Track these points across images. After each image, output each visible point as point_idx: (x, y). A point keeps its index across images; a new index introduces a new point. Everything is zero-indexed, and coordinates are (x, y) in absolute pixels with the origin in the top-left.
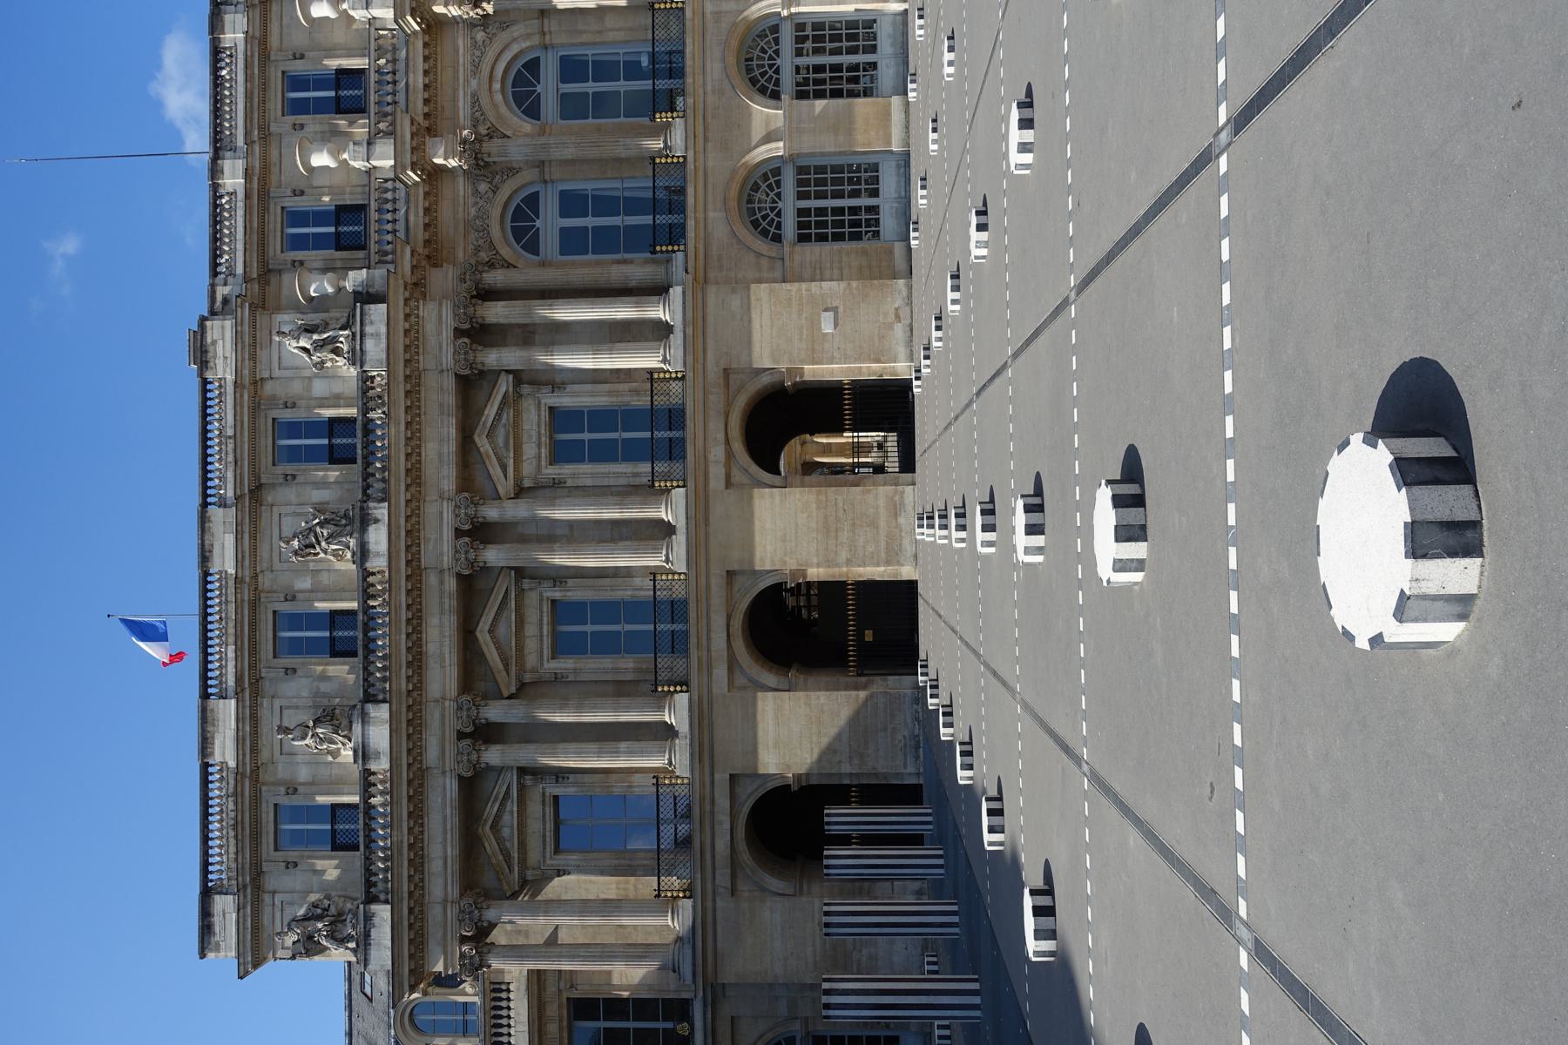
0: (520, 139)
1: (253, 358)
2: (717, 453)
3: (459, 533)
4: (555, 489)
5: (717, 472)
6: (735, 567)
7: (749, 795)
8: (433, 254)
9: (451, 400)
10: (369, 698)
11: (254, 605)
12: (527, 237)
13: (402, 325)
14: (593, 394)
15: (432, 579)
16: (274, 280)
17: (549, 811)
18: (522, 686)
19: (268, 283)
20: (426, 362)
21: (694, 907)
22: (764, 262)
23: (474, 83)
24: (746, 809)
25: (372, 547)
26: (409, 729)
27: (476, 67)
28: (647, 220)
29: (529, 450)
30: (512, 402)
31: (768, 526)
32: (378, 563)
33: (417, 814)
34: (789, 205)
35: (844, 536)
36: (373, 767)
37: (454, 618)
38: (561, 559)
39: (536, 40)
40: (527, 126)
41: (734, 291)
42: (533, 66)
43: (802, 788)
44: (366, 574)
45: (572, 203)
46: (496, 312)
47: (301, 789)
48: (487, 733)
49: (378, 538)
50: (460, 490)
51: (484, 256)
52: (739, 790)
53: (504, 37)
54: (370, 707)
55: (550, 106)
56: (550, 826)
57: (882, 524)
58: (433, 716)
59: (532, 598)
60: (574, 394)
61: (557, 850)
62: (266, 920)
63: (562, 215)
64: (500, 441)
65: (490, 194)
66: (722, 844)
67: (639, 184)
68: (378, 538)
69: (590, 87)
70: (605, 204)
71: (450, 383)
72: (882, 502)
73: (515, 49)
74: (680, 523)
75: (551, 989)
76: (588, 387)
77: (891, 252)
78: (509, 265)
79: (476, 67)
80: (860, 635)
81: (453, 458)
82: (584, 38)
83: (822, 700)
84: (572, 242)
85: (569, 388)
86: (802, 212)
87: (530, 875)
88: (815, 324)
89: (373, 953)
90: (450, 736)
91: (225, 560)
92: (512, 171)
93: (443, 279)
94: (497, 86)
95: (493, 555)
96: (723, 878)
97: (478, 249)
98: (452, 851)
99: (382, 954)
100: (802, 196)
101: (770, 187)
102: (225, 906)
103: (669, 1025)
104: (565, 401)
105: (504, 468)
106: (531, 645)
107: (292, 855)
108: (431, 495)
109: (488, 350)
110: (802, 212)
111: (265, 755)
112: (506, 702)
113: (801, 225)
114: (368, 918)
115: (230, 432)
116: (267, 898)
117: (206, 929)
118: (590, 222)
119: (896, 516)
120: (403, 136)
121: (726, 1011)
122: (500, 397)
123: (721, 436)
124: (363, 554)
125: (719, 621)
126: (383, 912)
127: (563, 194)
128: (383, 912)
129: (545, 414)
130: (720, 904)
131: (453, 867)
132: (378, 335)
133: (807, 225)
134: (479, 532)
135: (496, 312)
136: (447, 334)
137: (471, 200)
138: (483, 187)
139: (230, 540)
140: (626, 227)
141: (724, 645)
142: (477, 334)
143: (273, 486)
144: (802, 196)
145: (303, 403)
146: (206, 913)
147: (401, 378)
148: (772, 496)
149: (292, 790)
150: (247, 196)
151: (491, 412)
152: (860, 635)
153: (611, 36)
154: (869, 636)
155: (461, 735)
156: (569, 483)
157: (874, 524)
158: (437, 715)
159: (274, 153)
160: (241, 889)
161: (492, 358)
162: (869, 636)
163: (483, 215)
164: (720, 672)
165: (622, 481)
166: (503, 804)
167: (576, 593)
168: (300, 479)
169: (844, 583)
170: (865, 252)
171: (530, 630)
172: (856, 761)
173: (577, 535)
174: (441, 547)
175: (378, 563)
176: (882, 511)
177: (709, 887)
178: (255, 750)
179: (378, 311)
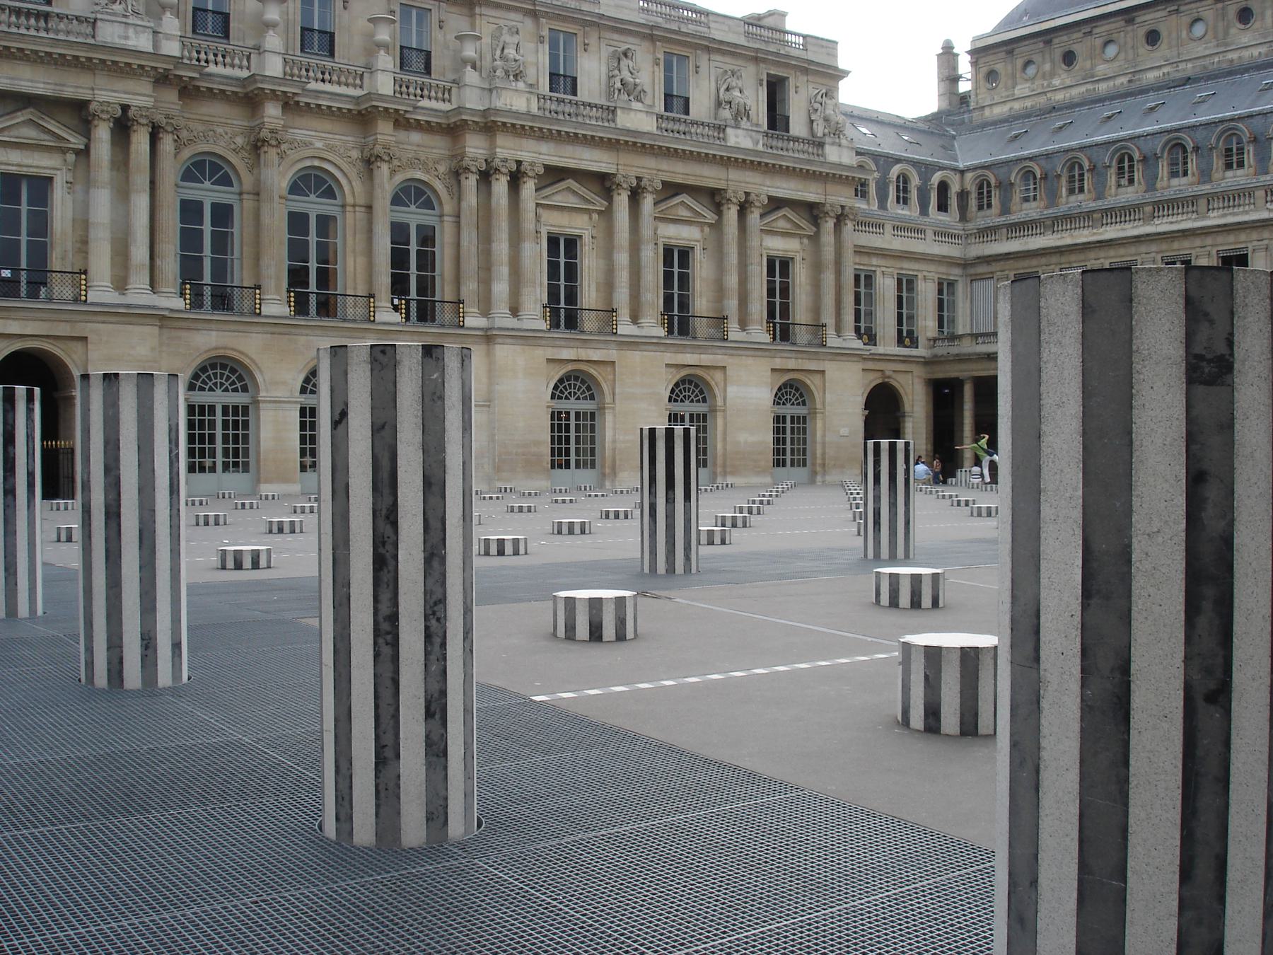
0: (278, 177)
8: (189, 91)
9: (68, 92)
13: (135, 62)
20: (101, 80)
23: (319, 144)
27: (330, 148)
28: (207, 279)
34: (219, 398)
39: (349, 200)
40: (285, 184)
41: (153, 349)
42: (330, 193)
45: (222, 214)
46: (140, 141)
51: (184, 134)
53: (353, 173)
63: (214, 205)
65: (233, 146)
67: (240, 275)
70: (222, 243)
71: (84, 95)
73: (343, 181)
78: (175, 156)
84: (190, 210)
86: (212, 409)
94: (316, 163)
100: (225, 409)
101: (233, 383)
109: (109, 132)
110: (212, 409)
113: (202, 407)
118: (207, 228)
120: (285, 85)
122: (65, 135)
129: (47, 173)
132: (127, 38)
133: (236, 413)
135: (140, 141)
138: (240, 141)
140: (201, 258)
147: (90, 55)
151: (52, 126)
161: (103, 133)
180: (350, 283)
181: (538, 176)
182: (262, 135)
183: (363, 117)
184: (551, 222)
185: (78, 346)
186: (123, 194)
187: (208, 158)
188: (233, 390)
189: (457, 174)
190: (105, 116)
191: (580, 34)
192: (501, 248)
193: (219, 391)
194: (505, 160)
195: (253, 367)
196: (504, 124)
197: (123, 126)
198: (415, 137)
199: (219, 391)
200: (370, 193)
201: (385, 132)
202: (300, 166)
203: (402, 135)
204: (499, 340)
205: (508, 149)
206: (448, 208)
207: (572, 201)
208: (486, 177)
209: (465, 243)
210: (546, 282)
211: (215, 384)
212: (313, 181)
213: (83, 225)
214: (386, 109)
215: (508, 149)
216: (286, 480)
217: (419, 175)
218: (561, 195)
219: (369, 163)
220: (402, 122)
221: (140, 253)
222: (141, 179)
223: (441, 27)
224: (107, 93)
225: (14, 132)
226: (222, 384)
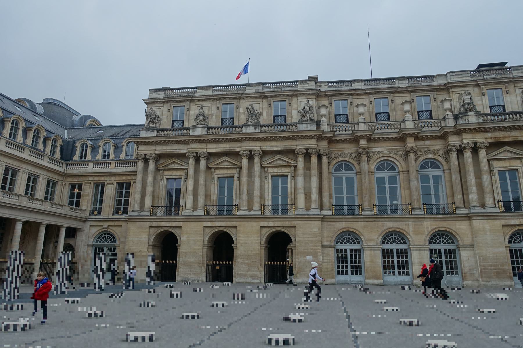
1: (303, 95)
2: (271, 224)
3: (251, 151)
4: (263, 178)
5: (265, 224)
6: (238, 229)
7: (176, 232)
9: (288, 148)
10: (208, 129)
11: (235, 98)
12: (340, 167)
14: (291, 188)
15: (239, 144)
16: (326, 98)
17: (178, 177)
18: (210, 169)
19: (325, 97)
22: (329, 239)
23: (386, 152)
24: (173, 231)
25: (248, 128)
26: (200, 140)
27: (391, 152)
29: (276, 170)
30: (289, 166)
32: (244, 130)
33: (177, 142)
34: (348, 246)
35: (246, 262)
36: (191, 130)
37: (228, 151)
38: (244, 179)
40: (373, 167)
41: (319, 229)
42: (393, 169)
43: (177, 247)
44: (241, 127)
45: (350, 181)
46: (314, 160)
47: (188, 112)
48: (197, 160)
49: (251, 129)
50: (262, 151)
51: (333, 156)
52: (178, 229)
53: (401, 160)
54: (206, 129)
55: (380, 174)
56: (174, 177)
57: (249, 273)
58: (203, 146)
59: (234, 171)
60: (291, 183)
61: (168, 179)
62: (157, 105)
64: (279, 162)
66: (163, 224)
68: (251, 129)
69: (387, 186)
71: (293, 148)
72: (255, 273)
73: (398, 163)
74: (252, 213)
75: (134, 178)
76: (293, 186)
77: (333, 278)
78: (329, 164)
79: (391, 152)
80: (218, 265)
81: (272, 149)
82: (402, 184)
84: (339, 181)
85: (293, 181)
87: (162, 172)
88: (309, 254)
89: (144, 132)
90: (197, 150)
91: (248, 90)
92: (359, 164)
93: (324, 145)
94: (386, 158)
95: (245, 161)
96: (154, 224)
97: (335, 154)
98: (168, 152)
99: (143, 134)
100: (351, 250)
102: (161, 95)
103: (122, 209)
104: (290, 179)
105: (270, 163)
106: (222, 171)
107: (171, 110)
108: (262, 144)
111: (197, 103)
112: (205, 165)
114: (153, 131)
115: (283, 89)
116: (162, 105)
117: (156, 90)
121: (123, 224)
123: (276, 225)
124: (246, 125)
125: (223, 224)
126: (154, 134)
127: (353, 178)
128: (154, 134)
131: (164, 152)
134: (251, 157)
135: (314, 160)
136: (307, 147)
137: (350, 152)
139: (254, 91)
141: (216, 225)
142: (307, 155)
143: (268, 101)
144: (351, 250)
145: (290, 108)
146: (159, 90)
148: (258, 240)
149: (188, 110)
150: (349, 90)
151: (286, 159)
152: (218, 265)
153: (403, 192)
154: (218, 268)
155: (197, 153)
156: (266, 181)
157: (249, 270)
158: (203, 147)
159: (363, 97)
160: (164, 98)
161: (301, 159)
162: (218, 268)
163: (345, 155)
164: (209, 224)
165: (266, 196)
166: (180, 164)
167: (236, 183)
168: (269, 108)
170: (332, 270)
171: (226, 171)
172: (182, 263)
173: (251, 184)
174: (247, 147)
175: (244, 130)
176: (253, 273)
177: (152, 220)
178: (198, 100)
179: (314, 127)
180: (404, 201)
181: (487, 147)
182: (359, 151)
183: (402, 138)
184: (499, 166)
185: (293, 229)
186: (307, 177)
187: (343, 163)
188: (400, 243)
189: (448, 152)
190: (301, 153)
191: (504, 88)
192: (472, 179)
193: (348, 244)
194: (468, 143)
195: (360, 234)
196: (465, 129)
197: (307, 155)
198: (428, 142)
199: (348, 244)
200: (408, 166)
201: (411, 142)
202: (379, 160)
203: (421, 143)
204: (474, 218)
205: (469, 139)
206: (446, 167)
207: (509, 155)
208: (460, 152)
209: (454, 180)
210: (500, 191)
211: (443, 241)
212: (386, 165)
213: (296, 189)
214: (409, 134)
215: (469, 139)
216: (377, 278)
217: (430, 156)
218: (504, 153)
219: (406, 154)
220: (417, 138)
221: (315, 196)
222: (314, 172)
223: (435, 101)
224: (302, 145)
225: (275, 163)
226: (349, 241)
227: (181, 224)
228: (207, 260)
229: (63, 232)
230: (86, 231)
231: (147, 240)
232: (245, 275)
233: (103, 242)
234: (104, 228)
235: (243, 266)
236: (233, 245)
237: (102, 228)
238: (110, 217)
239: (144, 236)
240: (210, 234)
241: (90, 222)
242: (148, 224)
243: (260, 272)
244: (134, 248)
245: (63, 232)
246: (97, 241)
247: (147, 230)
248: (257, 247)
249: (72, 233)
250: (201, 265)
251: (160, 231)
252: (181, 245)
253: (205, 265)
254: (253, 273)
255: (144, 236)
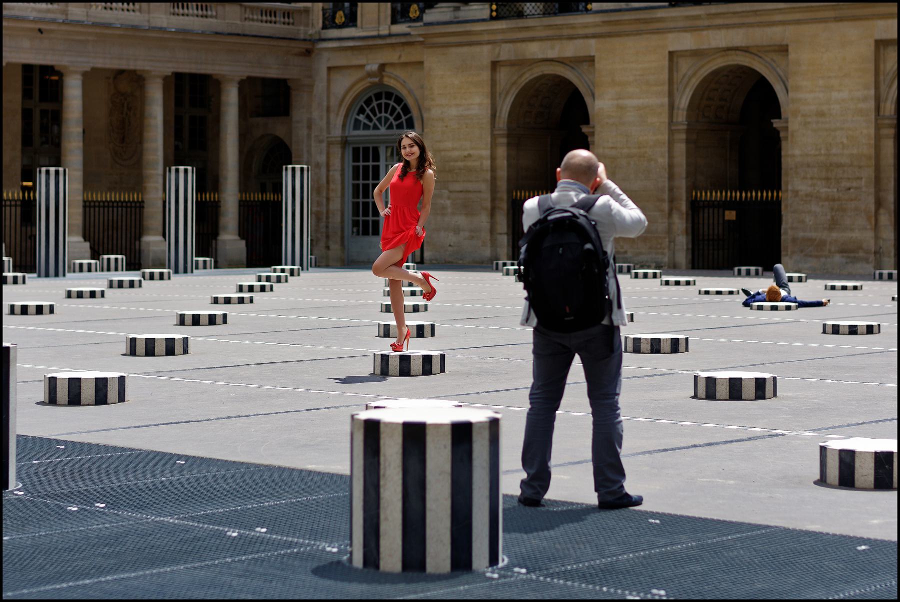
6: (792, 55)
21: (484, 20)
31: (835, 95)
57: (834, 235)
66: (534, 50)
72: (856, 235)
83: (660, 160)
96: (506, 52)
119: (842, 251)
125: (736, 37)
130: (486, 49)
148: (865, 99)
154: (731, 215)
157: (833, 225)
162: (731, 215)
169: (779, 188)
176: (848, 235)
227: (592, 47)
228: (692, 186)
229: (231, 98)
230: (320, 86)
231: (486, 113)
232: (821, 244)
233: (375, 127)
234: (370, 75)
235: (814, 208)
236: (776, 123)
237: (358, 75)
238: (384, 31)
239: (477, 100)
240: (695, 82)
241: (326, 55)
242: (485, 54)
243: (876, 227)
244: (449, 145)
245: (231, 98)
246: (357, 125)
247: (486, 75)
248: (865, 129)
249: (271, 99)
250: (666, 206)
251: (528, 77)
252: (598, 129)
253: (683, 206)
254: (848, 235)
255: (477, 100)
